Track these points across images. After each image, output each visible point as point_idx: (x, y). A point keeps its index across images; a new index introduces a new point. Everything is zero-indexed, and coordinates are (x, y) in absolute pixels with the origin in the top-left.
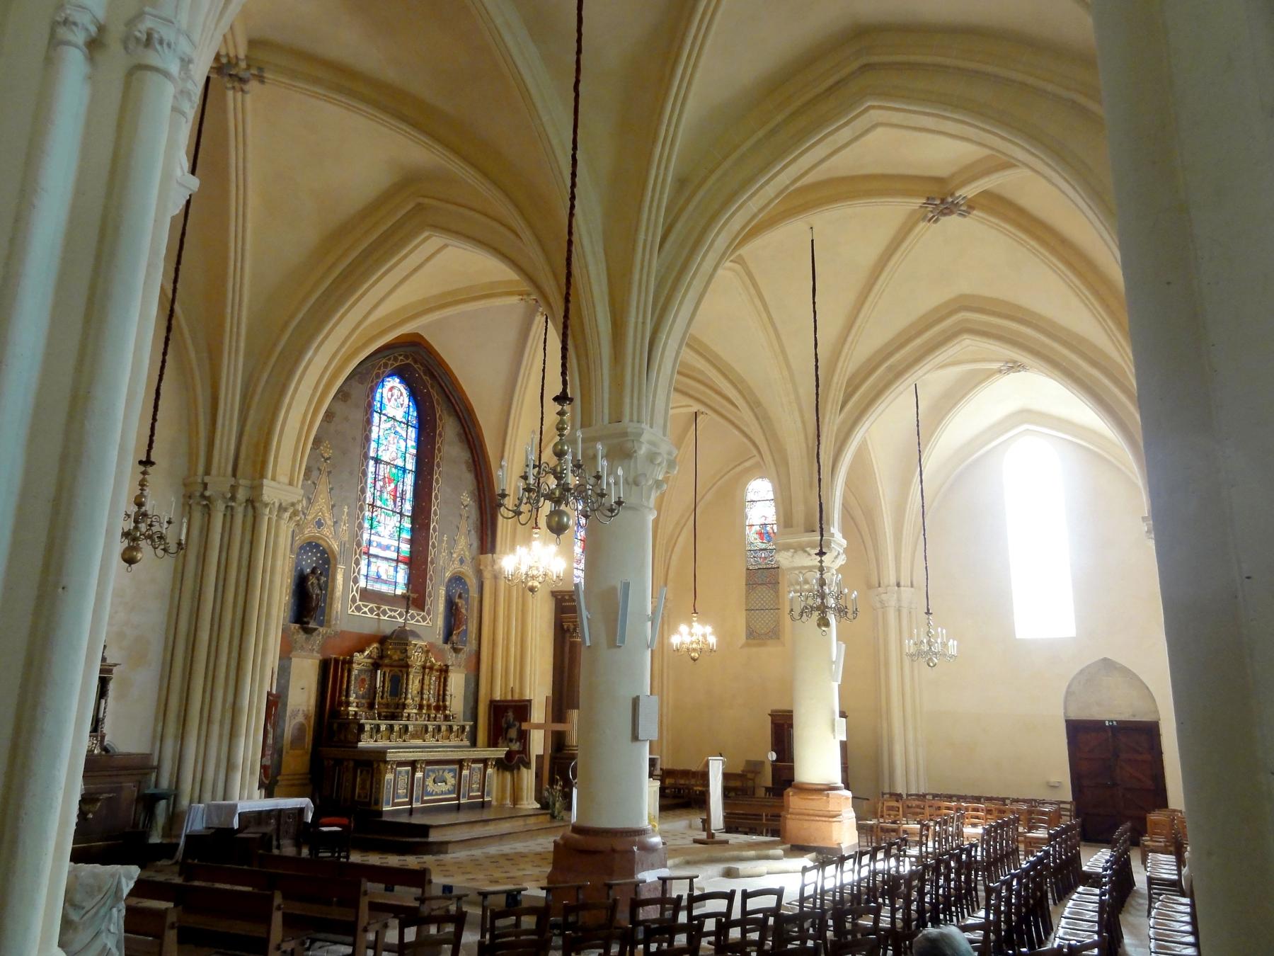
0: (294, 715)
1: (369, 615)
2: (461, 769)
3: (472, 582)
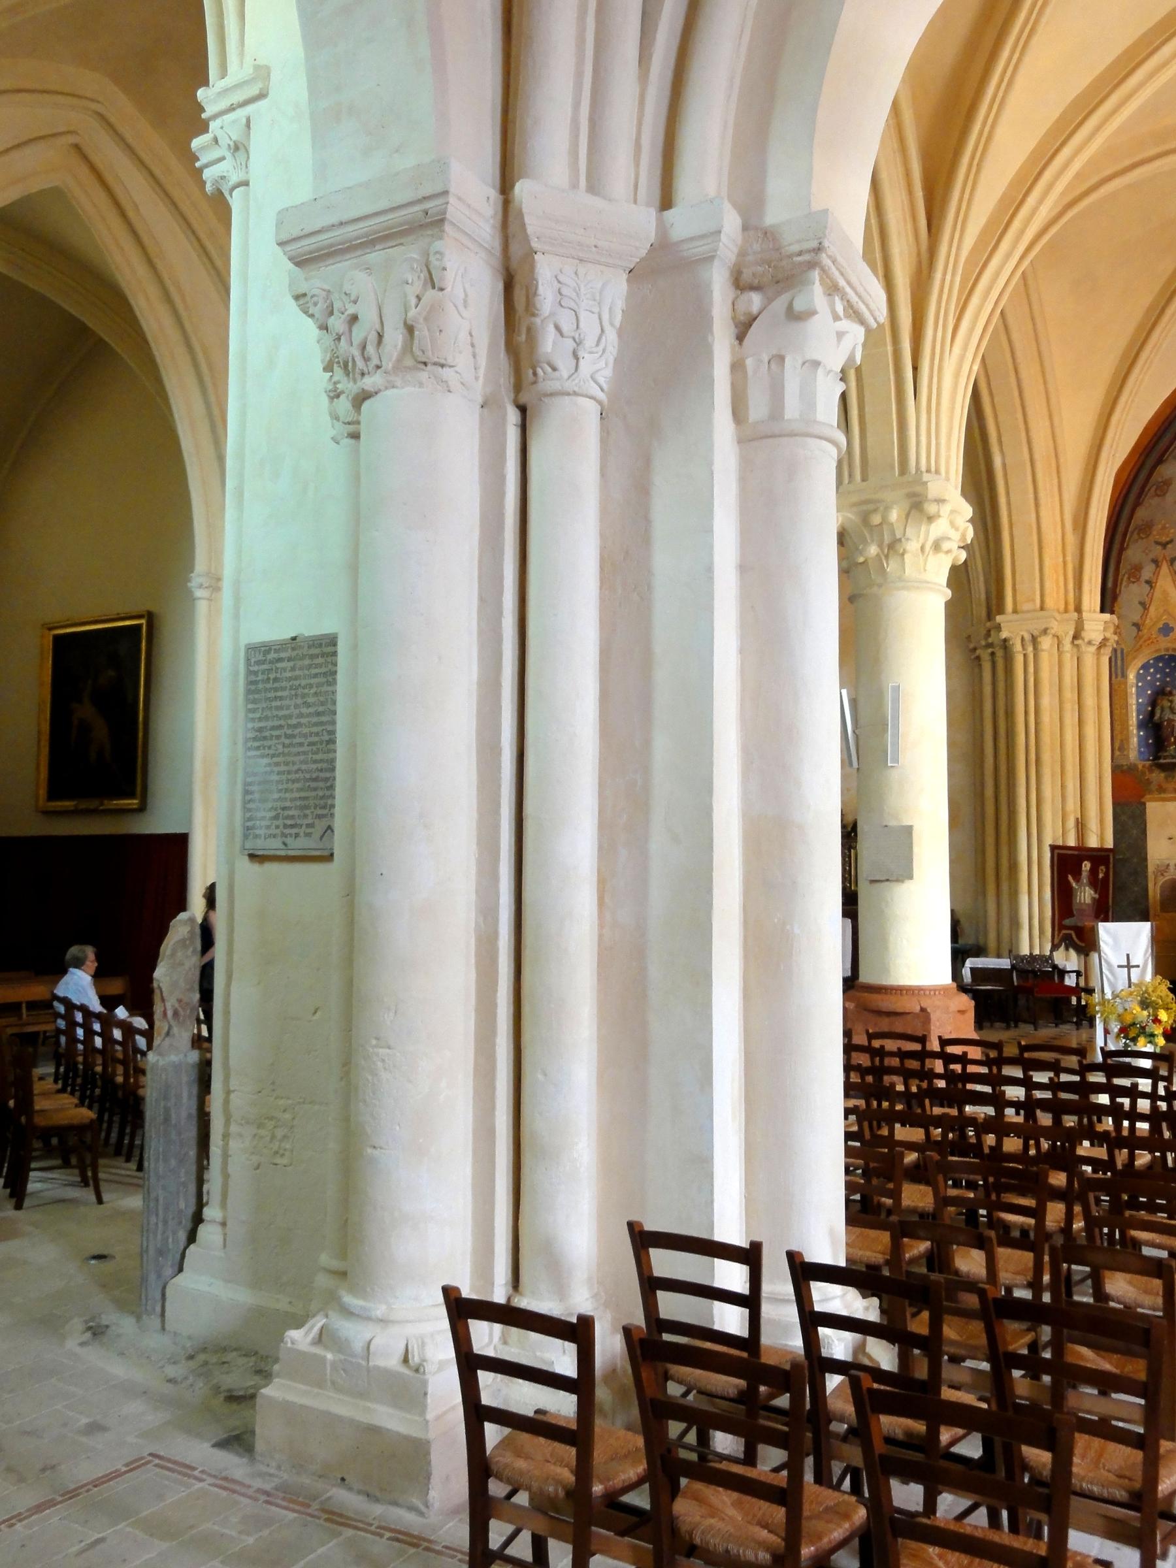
0: (1163, 869)
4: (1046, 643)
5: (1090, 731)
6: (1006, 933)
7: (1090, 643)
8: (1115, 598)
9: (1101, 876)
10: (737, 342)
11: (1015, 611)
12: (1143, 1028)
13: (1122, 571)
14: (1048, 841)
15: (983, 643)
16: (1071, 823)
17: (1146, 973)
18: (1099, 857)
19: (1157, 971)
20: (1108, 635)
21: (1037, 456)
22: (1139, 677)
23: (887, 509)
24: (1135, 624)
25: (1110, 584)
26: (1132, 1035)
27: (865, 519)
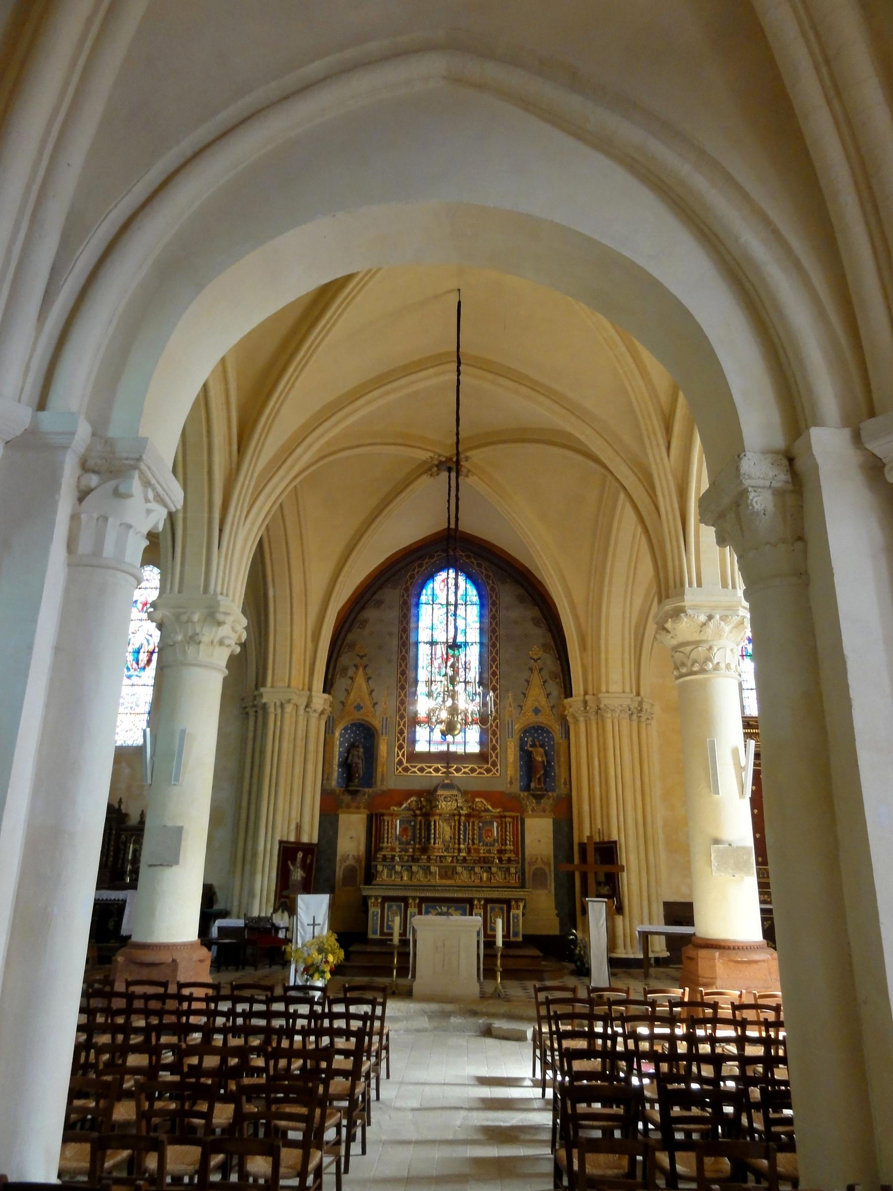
0: (345, 858)
1: (420, 774)
2: (509, 909)
3: (556, 728)
4: (289, 708)
5: (310, 767)
6: (244, 901)
7: (315, 711)
8: (332, 685)
9: (308, 861)
10: (77, 502)
11: (272, 686)
12: (318, 967)
13: (337, 670)
14: (278, 838)
15: (251, 704)
16: (293, 827)
17: (323, 930)
18: (308, 849)
19: (331, 927)
20: (326, 707)
21: (294, 595)
22: (341, 735)
23: (193, 613)
24: (342, 703)
25: (330, 676)
26: (310, 972)
27: (177, 616)
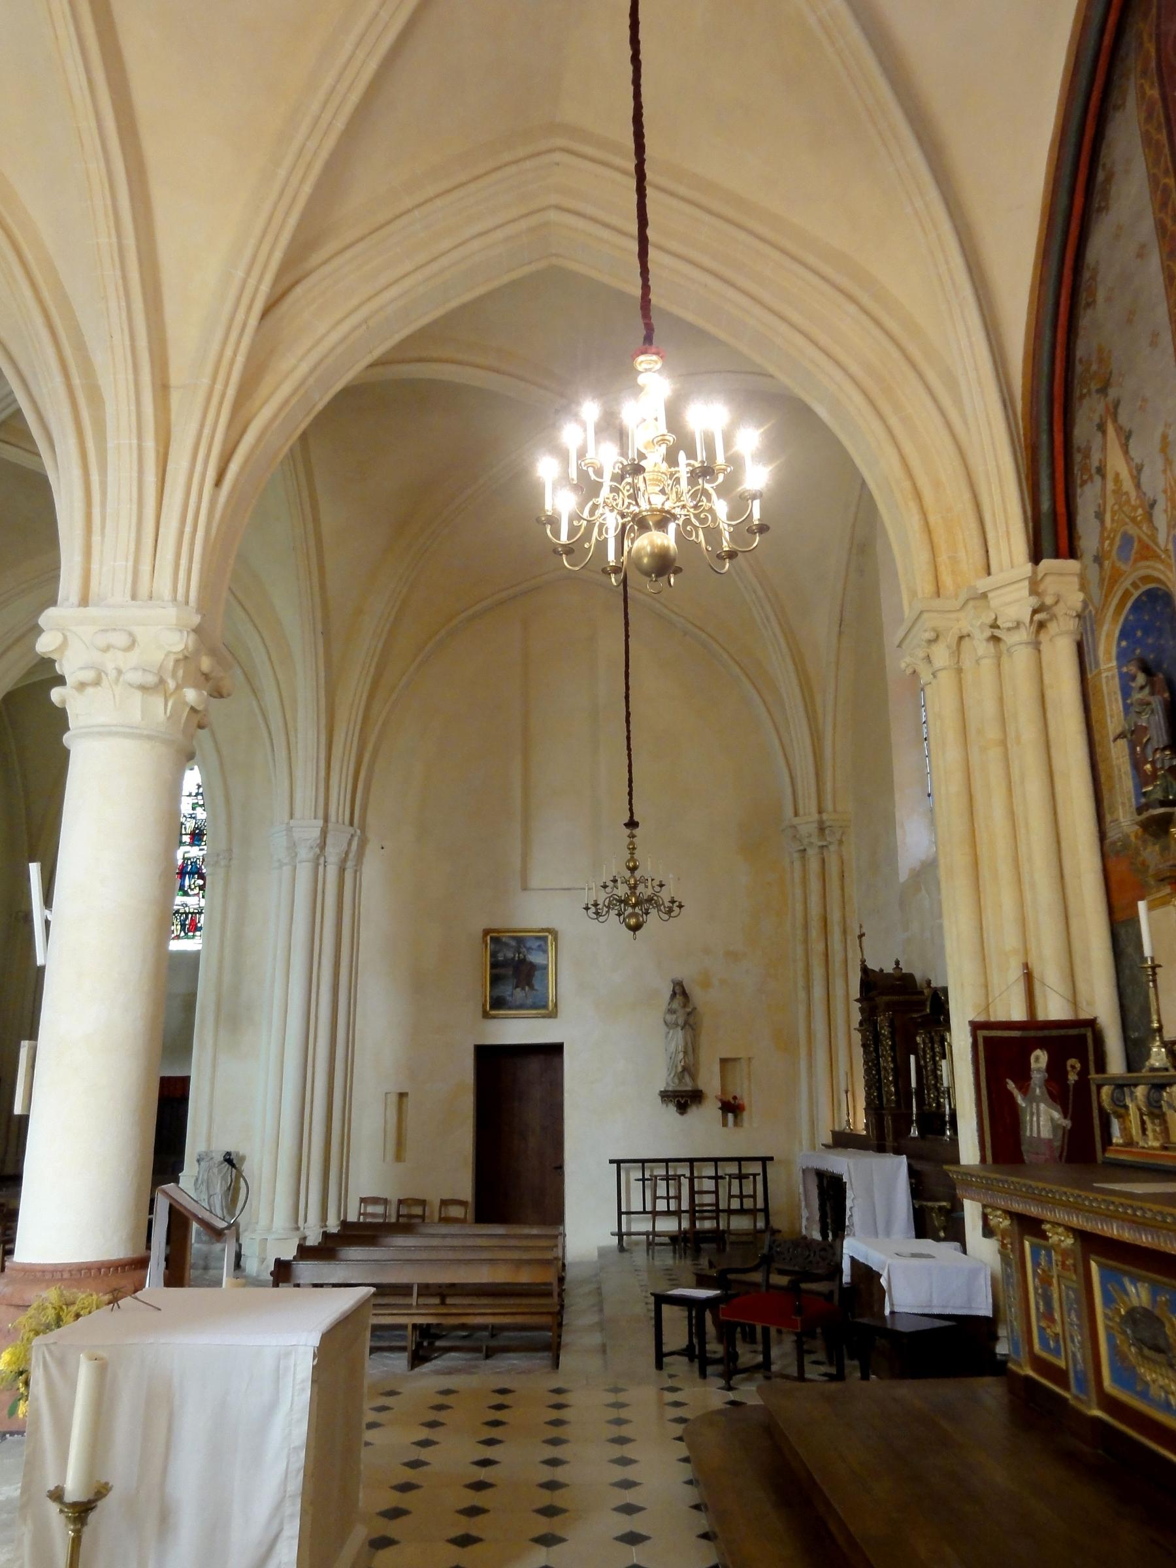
9: (1072, 1078)
18: (1074, 1040)
